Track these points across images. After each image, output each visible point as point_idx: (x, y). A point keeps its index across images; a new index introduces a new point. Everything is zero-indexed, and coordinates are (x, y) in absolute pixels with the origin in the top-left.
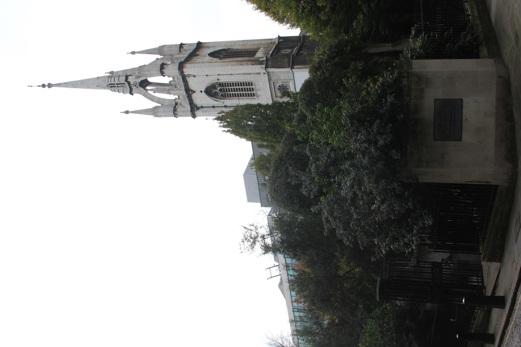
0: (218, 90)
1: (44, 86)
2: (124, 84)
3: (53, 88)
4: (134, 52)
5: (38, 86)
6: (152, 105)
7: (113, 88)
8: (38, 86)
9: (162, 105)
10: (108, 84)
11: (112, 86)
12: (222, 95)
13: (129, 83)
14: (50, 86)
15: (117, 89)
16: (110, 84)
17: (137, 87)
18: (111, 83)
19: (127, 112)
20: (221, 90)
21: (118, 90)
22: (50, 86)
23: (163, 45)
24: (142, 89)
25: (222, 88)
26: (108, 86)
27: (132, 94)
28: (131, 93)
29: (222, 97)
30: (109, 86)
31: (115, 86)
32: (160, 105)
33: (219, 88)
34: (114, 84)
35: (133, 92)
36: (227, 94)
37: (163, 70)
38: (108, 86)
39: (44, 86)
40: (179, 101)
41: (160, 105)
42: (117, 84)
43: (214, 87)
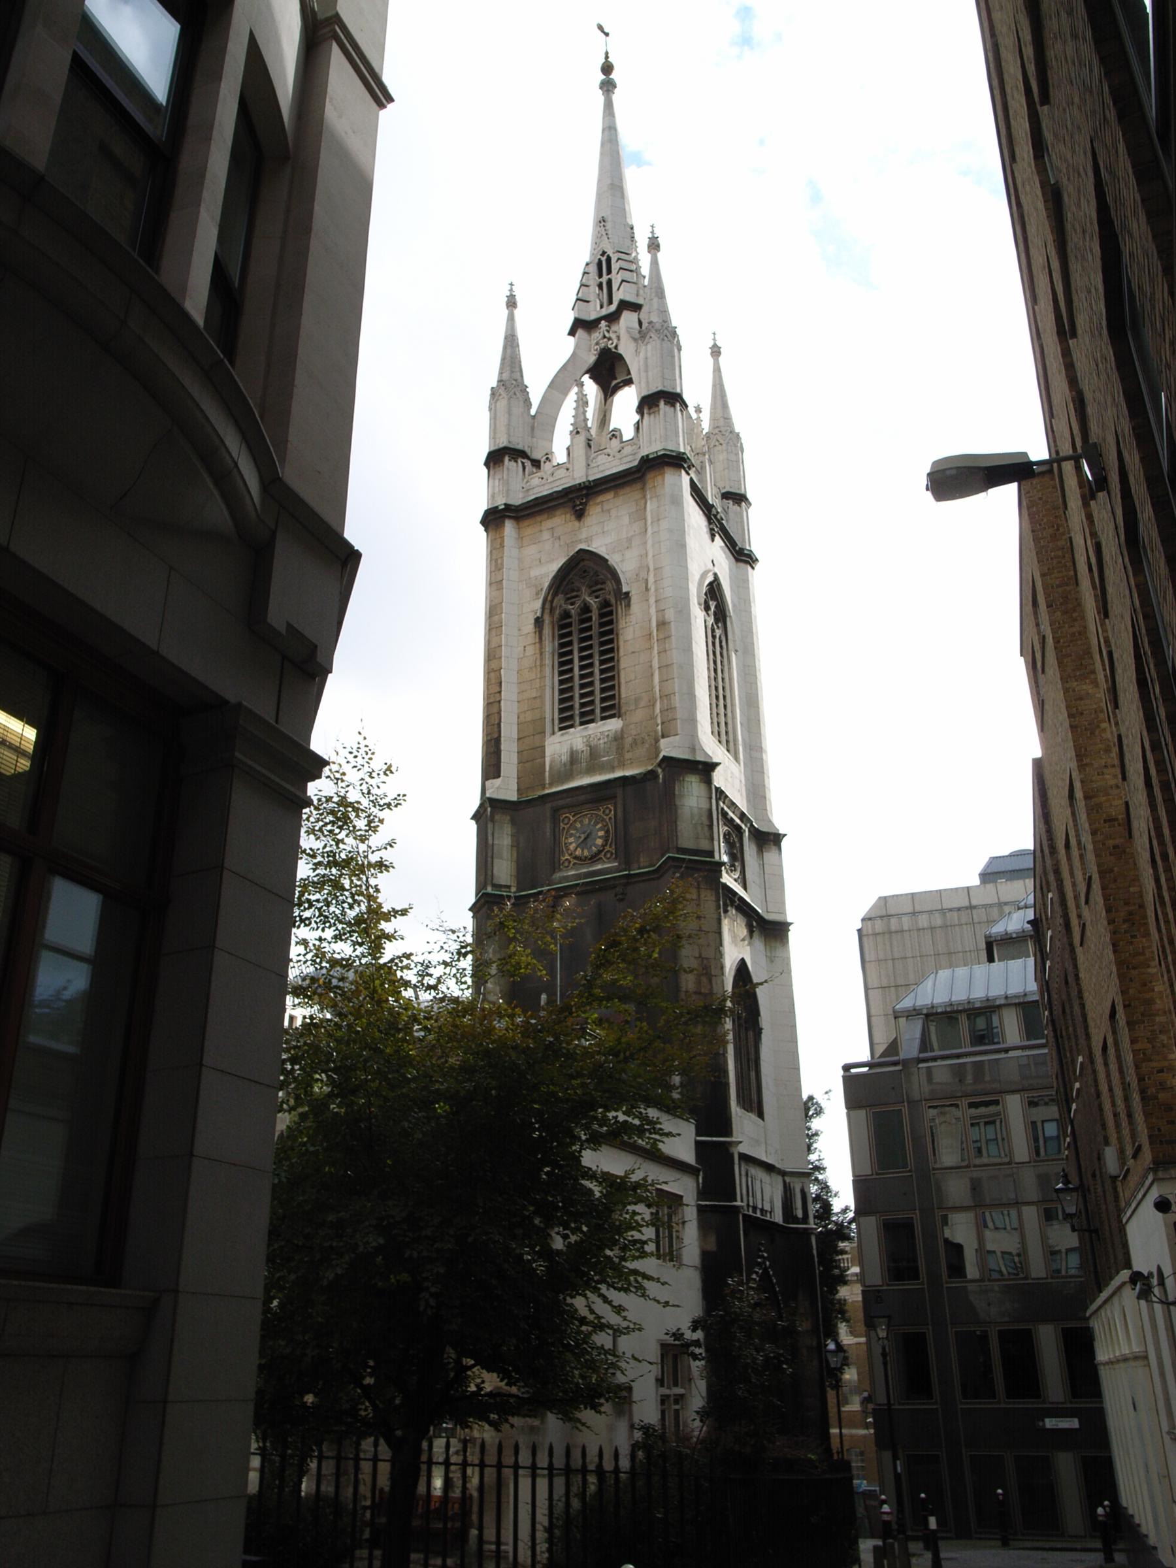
0: (588, 599)
1: (607, 68)
2: (610, 302)
3: (600, 97)
4: (720, 353)
5: (607, 53)
6: (537, 383)
7: (593, 269)
8: (607, 53)
9: (534, 417)
10: (610, 252)
11: (602, 265)
12: (566, 615)
13: (612, 318)
14: (608, 86)
15: (593, 279)
16: (609, 260)
17: (597, 344)
18: (613, 261)
19: (512, 303)
20: (586, 609)
21: (588, 302)
22: (608, 86)
23: (744, 446)
24: (592, 359)
25: (591, 612)
26: (604, 253)
27: (572, 332)
28: (579, 325)
29: (560, 615)
30: (604, 259)
31: (600, 276)
32: (533, 412)
33: (593, 602)
34: (609, 271)
35: (580, 333)
36: (570, 634)
37: (662, 403)
38: (604, 253)
39: (607, 68)
40: (546, 467)
41: (533, 412)
42: (609, 282)
43: (597, 583)
